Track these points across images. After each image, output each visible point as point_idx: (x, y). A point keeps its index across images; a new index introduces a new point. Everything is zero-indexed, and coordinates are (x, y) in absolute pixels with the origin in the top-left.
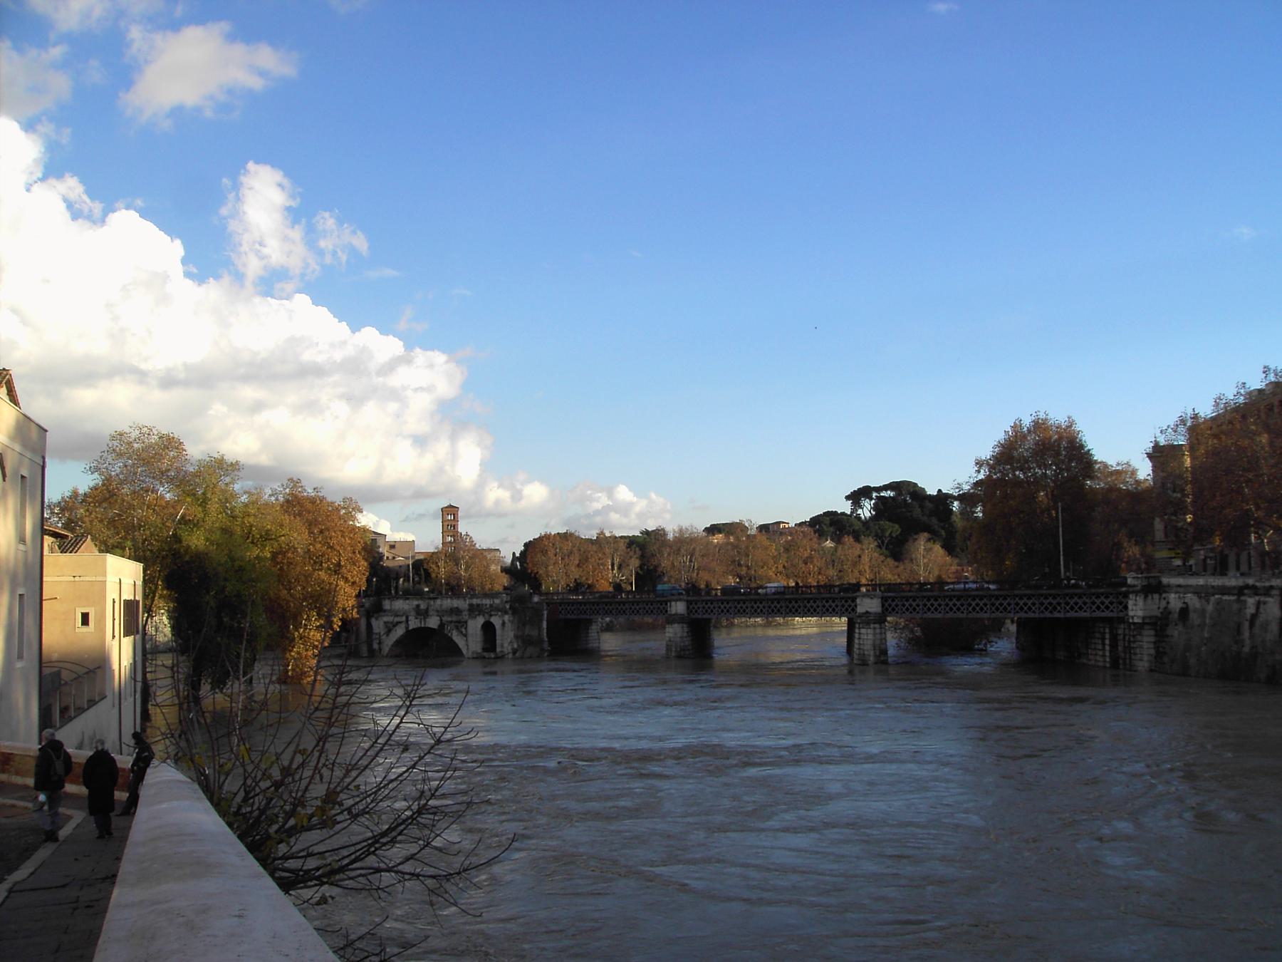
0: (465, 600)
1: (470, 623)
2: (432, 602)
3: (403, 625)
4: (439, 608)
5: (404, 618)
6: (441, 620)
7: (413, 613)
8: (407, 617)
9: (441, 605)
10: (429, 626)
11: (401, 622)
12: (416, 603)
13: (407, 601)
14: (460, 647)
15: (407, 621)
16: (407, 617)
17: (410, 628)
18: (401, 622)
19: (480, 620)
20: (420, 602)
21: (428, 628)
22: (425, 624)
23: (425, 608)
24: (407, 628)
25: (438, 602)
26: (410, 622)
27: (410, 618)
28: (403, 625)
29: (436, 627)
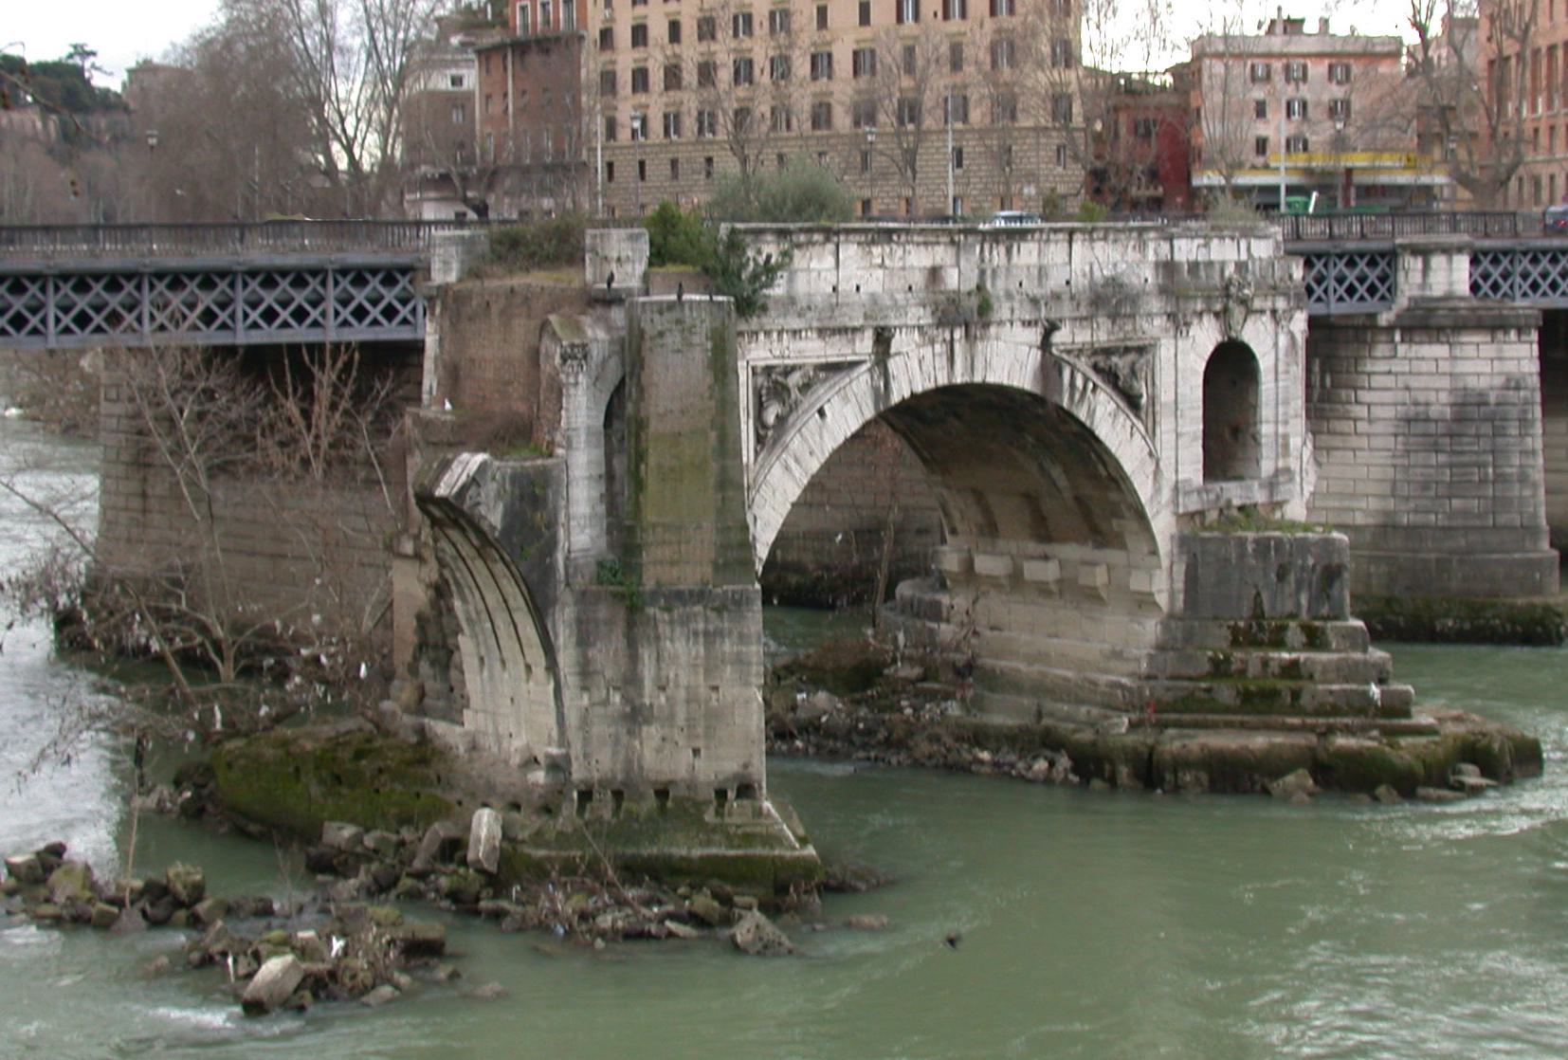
0: (1142, 246)
1: (1165, 351)
2: (998, 256)
3: (861, 382)
4: (1031, 288)
5: (865, 345)
6: (1045, 345)
9: (1042, 272)
10: (992, 379)
12: (920, 258)
13: (876, 250)
14: (1128, 466)
16: (883, 339)
17: (899, 392)
19: (1205, 337)
20: (942, 254)
21: (985, 388)
23: (971, 284)
24: (881, 394)
25: (1027, 253)
26: (894, 365)
28: (861, 382)
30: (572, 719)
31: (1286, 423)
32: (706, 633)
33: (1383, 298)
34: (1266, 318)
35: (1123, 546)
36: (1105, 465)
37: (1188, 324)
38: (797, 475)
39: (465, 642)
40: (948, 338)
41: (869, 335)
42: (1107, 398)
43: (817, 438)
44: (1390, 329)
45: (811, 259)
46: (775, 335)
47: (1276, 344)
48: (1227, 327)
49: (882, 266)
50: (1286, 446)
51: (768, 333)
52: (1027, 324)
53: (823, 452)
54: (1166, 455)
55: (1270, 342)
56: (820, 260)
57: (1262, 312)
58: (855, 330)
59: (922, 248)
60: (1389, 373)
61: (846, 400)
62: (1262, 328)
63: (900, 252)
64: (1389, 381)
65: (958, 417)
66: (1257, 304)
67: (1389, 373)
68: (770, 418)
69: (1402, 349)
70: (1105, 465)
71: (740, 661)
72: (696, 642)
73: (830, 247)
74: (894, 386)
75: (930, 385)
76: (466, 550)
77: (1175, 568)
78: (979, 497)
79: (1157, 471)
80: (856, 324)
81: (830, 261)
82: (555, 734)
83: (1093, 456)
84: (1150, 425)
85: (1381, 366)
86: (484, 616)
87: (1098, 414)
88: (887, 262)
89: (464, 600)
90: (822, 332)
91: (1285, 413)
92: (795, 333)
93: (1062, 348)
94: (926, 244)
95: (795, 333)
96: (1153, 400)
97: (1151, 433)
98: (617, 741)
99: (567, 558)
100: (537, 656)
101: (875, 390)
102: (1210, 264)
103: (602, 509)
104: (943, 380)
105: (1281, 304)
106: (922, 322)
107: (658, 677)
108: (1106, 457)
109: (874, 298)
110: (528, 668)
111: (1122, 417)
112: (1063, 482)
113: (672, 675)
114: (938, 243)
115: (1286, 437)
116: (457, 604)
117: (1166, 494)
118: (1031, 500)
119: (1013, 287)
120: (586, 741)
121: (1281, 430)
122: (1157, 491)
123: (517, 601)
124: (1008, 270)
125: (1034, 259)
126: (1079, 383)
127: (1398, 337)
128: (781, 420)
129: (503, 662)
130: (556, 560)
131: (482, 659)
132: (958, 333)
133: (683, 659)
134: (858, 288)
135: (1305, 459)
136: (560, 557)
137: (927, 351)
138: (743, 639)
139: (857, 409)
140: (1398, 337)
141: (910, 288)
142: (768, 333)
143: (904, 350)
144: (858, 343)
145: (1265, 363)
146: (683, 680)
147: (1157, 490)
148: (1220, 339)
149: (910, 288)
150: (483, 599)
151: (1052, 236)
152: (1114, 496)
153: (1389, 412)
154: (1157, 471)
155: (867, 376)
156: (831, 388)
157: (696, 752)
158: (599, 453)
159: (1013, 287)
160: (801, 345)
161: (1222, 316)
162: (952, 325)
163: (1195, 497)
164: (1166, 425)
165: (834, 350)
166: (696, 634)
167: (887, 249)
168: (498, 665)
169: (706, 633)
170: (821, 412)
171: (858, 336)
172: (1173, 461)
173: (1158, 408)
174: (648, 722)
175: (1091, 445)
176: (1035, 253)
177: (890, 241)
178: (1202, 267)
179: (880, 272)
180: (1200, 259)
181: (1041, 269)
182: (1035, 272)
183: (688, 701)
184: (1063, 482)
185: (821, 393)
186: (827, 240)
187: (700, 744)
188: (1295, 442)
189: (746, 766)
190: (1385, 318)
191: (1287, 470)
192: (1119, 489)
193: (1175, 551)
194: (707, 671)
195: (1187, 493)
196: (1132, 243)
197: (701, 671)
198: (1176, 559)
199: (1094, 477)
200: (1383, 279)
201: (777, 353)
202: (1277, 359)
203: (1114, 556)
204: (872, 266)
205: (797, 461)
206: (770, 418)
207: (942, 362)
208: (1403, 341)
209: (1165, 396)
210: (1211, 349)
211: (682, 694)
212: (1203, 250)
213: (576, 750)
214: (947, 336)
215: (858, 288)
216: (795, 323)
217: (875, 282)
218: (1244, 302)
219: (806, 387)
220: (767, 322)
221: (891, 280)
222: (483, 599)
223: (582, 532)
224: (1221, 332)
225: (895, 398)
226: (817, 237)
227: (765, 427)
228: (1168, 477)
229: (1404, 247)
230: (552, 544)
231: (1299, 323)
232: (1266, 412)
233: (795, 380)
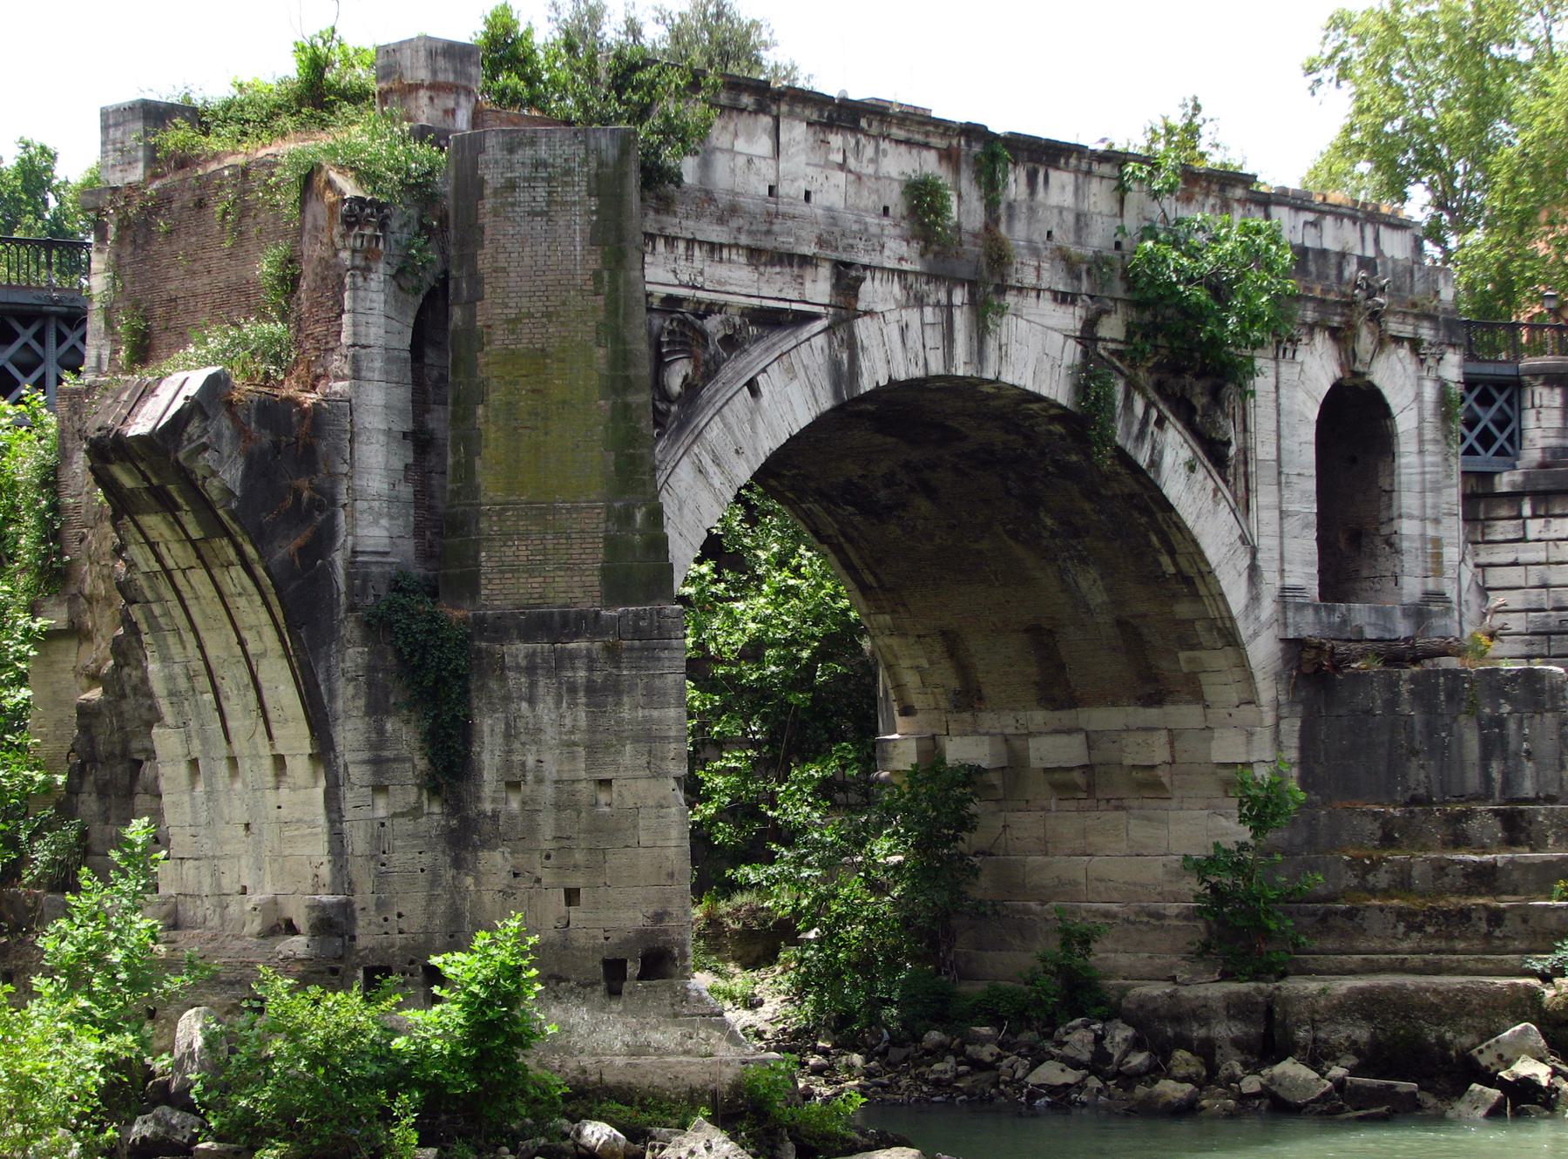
4: (1064, 238)
5: (818, 289)
7: (897, 250)
8: (847, 279)
9: (1081, 220)
10: (1008, 378)
11: (774, 320)
13: (836, 140)
15: (846, 310)
16: (847, 279)
17: (873, 374)
18: (774, 320)
22: (979, 355)
24: (843, 373)
26: (864, 329)
27: (874, 292)
29: (1056, 388)
30: (358, 841)
31: (1437, 521)
32: (591, 689)
33: (1501, 452)
34: (1404, 352)
35: (1198, 697)
36: (1172, 553)
37: (1294, 341)
38: (717, 481)
39: (167, 742)
40: (944, 300)
41: (825, 271)
42: (1179, 439)
43: (747, 426)
44: (1514, 497)
45: (736, 135)
46: (682, 246)
47: (1419, 396)
48: (1348, 355)
49: (842, 167)
50: (1438, 557)
51: (671, 241)
52: (1063, 298)
53: (756, 455)
54: (1267, 544)
55: (1410, 392)
56: (750, 137)
57: (1398, 340)
58: (805, 261)
59: (903, 149)
60: (1515, 564)
61: (791, 373)
62: (1399, 367)
63: (869, 151)
64: (1514, 576)
65: (931, 492)
66: (1394, 326)
67: (1515, 564)
68: (675, 383)
69: (1535, 527)
70: (1172, 553)
71: (649, 737)
72: (573, 704)
73: (766, 121)
74: (864, 364)
75: (918, 373)
76: (177, 554)
77: (1284, 726)
78: (952, 644)
79: (1254, 571)
80: (809, 249)
81: (763, 145)
82: (325, 871)
83: (1154, 539)
84: (1241, 492)
85: (1504, 554)
86: (203, 682)
87: (1168, 460)
88: (852, 163)
89: (166, 659)
90: (756, 256)
91: (1435, 506)
92: (714, 248)
93: (1111, 346)
94: (908, 143)
95: (714, 248)
96: (1245, 451)
97: (1243, 506)
98: (434, 882)
99: (351, 563)
100: (295, 737)
101: (835, 365)
102: (1323, 253)
103: (406, 491)
104: (936, 368)
105: (1426, 333)
106: (906, 266)
107: (507, 764)
108: (1176, 538)
109: (832, 215)
110: (279, 762)
111: (1200, 474)
112: (1097, 596)
113: (531, 761)
114: (927, 146)
115: (1437, 542)
116: (153, 667)
117: (1268, 608)
118: (1042, 638)
119: (1039, 238)
120: (382, 878)
121: (1431, 531)
122: (1255, 599)
123: (265, 639)
124: (1032, 210)
125: (1068, 199)
126: (1139, 406)
127: (1527, 510)
128: (692, 389)
129: (233, 761)
130: (332, 564)
131: (194, 764)
132: (959, 296)
133: (550, 735)
134: (808, 195)
135: (1465, 584)
136: (339, 559)
137: (913, 316)
138: (654, 697)
139: (808, 391)
140: (1527, 510)
141: (886, 210)
142: (671, 241)
143: (878, 308)
144: (808, 284)
145: (1405, 422)
146: (551, 770)
147: (1255, 599)
148: (1339, 374)
149: (886, 210)
150: (201, 647)
151: (1095, 166)
152: (1184, 609)
153: (1517, 623)
154: (1254, 571)
155: (820, 341)
156: (767, 349)
157: (572, 896)
158: (403, 394)
159: (1039, 238)
160: (721, 271)
161: (1342, 337)
162: (953, 281)
163: (1309, 615)
164: (1264, 496)
165: (773, 289)
166: (573, 689)
167: (852, 142)
168: (222, 768)
169: (591, 689)
170: (753, 387)
171: (809, 273)
172: (1277, 556)
173: (1252, 468)
174: (488, 844)
175: (1151, 514)
176: (1070, 189)
177: (855, 129)
178: (1311, 256)
179: (840, 177)
180: (1308, 244)
181: (1079, 216)
182: (1070, 219)
183: (558, 807)
184: (1097, 596)
185: (754, 359)
186: (761, 109)
187: (576, 880)
188: (1451, 554)
189: (659, 917)
190: (1505, 482)
191: (1440, 596)
192: (1195, 596)
193: (1282, 698)
194: (591, 749)
195: (1300, 607)
196: (1211, 201)
197: (581, 751)
198: (1284, 711)
199: (1156, 578)
200: (1502, 424)
201: (685, 278)
202: (1421, 420)
203: (1184, 715)
204: (827, 164)
205: (717, 461)
206: (675, 383)
207: (934, 338)
208: (1535, 516)
209: (1264, 450)
210: (1328, 387)
211: (548, 792)
212: (1312, 231)
213: (364, 897)
214: (943, 296)
215: (808, 195)
216: (716, 234)
217: (833, 191)
218: (1375, 316)
219: (732, 343)
220: (672, 225)
221: (858, 193)
222: (201, 647)
223: (376, 522)
224: (1342, 366)
225: (866, 385)
226: (747, 100)
227: (665, 396)
228: (1271, 582)
229: (1535, 373)
230: (324, 539)
231: (1452, 367)
232: (1408, 501)
233: (713, 324)
